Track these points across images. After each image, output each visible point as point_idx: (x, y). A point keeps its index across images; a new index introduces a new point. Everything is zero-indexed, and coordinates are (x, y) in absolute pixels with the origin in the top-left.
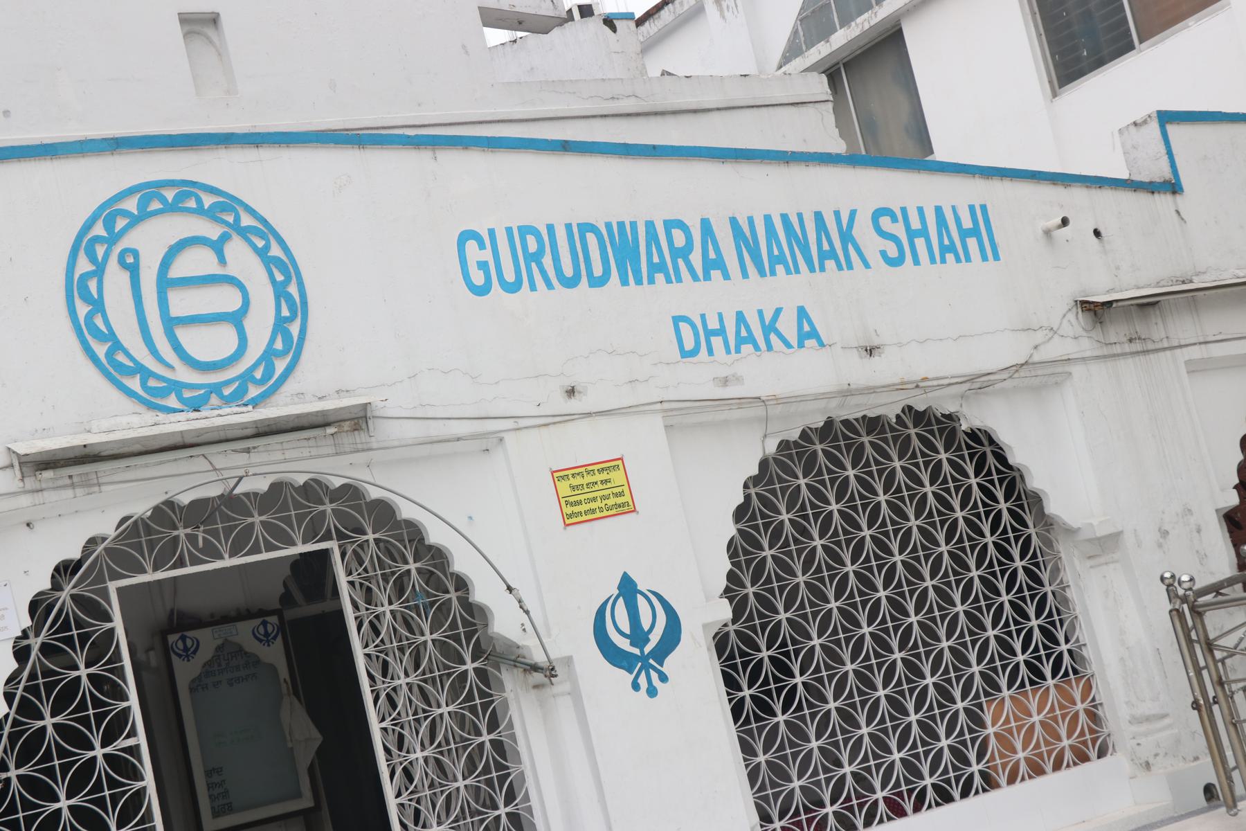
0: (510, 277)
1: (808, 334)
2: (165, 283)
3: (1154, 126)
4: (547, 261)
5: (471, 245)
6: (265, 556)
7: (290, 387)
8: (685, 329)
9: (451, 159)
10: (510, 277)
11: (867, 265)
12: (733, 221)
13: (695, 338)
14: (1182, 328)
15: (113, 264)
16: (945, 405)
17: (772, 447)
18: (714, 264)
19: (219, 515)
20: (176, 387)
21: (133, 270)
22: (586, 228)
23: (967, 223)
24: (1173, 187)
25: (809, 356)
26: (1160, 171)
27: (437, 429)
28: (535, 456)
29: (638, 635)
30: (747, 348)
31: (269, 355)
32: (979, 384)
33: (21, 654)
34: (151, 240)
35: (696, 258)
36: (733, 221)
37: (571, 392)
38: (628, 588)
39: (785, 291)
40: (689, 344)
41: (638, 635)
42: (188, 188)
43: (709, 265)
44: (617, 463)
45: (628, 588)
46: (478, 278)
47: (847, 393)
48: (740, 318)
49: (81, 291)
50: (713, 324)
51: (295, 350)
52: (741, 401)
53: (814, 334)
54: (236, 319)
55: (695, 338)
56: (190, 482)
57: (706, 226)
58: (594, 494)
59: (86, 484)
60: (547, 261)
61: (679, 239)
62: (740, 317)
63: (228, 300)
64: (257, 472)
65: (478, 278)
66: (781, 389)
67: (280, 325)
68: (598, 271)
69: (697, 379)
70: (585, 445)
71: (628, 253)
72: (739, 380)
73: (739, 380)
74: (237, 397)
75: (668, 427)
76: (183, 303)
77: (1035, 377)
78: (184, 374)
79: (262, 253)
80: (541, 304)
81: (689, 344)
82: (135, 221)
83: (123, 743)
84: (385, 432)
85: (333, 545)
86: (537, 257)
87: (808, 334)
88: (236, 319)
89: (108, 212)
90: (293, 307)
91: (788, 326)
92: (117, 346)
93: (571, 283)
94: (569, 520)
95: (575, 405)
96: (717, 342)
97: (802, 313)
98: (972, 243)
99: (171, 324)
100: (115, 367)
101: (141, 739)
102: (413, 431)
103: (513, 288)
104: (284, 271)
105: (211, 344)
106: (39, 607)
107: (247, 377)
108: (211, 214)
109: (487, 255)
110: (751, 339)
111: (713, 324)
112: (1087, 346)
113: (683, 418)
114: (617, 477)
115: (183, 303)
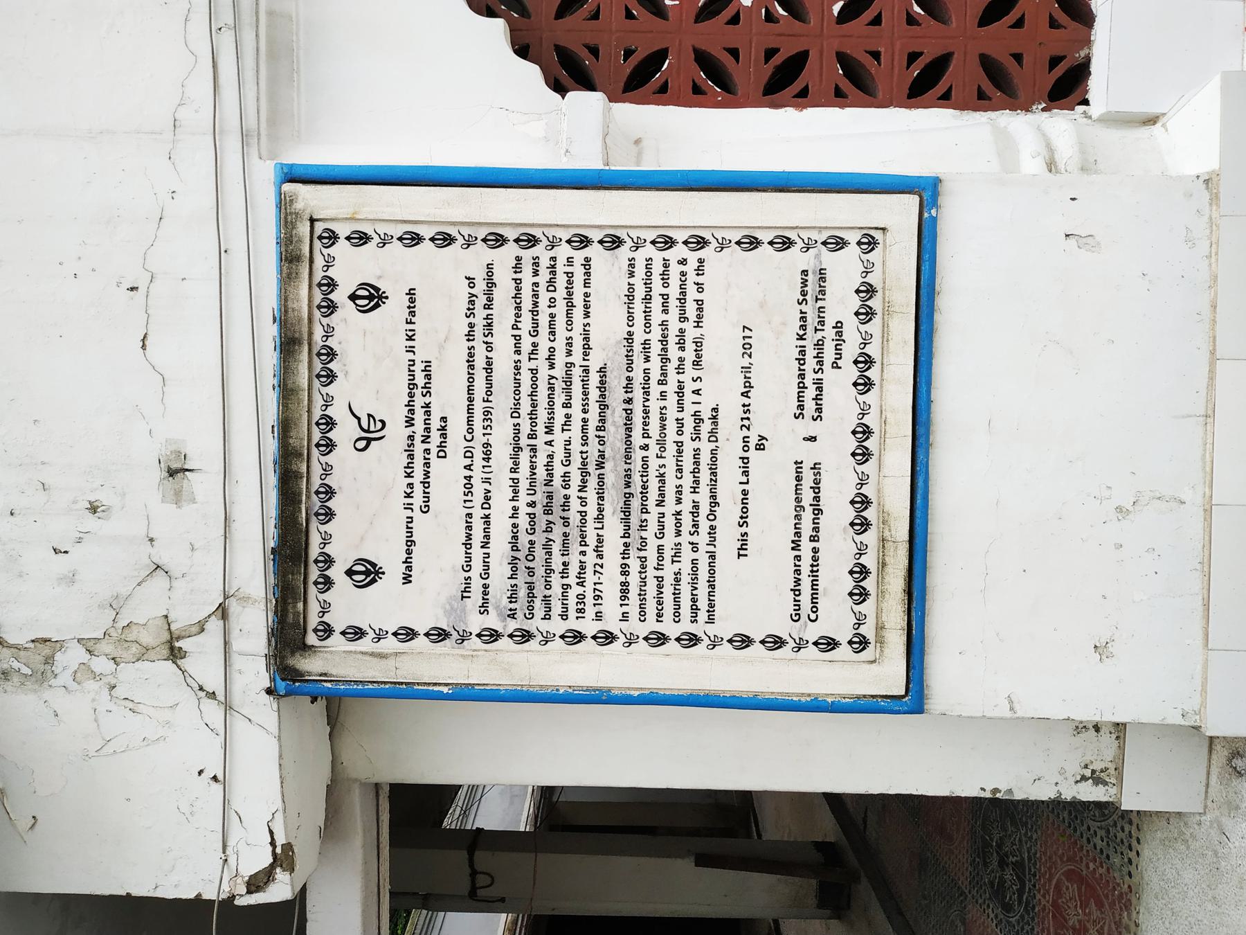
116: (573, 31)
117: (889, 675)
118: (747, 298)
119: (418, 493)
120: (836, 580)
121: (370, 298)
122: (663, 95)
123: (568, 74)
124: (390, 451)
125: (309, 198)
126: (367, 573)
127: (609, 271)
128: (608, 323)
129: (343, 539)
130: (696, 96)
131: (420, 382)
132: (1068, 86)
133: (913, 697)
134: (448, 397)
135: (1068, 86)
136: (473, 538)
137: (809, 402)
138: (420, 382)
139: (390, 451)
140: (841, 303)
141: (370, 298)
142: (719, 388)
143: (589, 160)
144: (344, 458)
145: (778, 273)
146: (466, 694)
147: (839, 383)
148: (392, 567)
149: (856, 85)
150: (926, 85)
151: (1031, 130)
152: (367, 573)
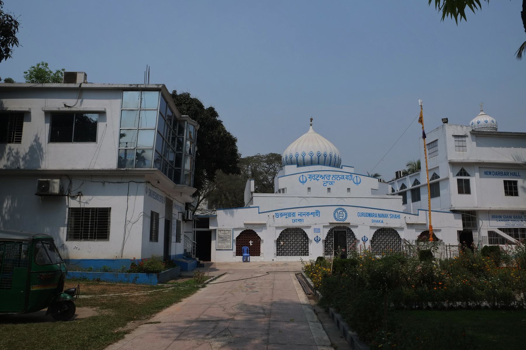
1: (382, 222)
13: (373, 221)
19: (340, 227)
24: (418, 215)
26: (417, 214)
32: (395, 228)
34: (339, 211)
39: (381, 219)
49: (334, 214)
55: (373, 221)
56: (338, 225)
64: (342, 225)
71: (370, 215)
77: (402, 229)
80: (363, 218)
100: (335, 218)
104: (346, 214)
118: (229, 244)
123: (237, 238)
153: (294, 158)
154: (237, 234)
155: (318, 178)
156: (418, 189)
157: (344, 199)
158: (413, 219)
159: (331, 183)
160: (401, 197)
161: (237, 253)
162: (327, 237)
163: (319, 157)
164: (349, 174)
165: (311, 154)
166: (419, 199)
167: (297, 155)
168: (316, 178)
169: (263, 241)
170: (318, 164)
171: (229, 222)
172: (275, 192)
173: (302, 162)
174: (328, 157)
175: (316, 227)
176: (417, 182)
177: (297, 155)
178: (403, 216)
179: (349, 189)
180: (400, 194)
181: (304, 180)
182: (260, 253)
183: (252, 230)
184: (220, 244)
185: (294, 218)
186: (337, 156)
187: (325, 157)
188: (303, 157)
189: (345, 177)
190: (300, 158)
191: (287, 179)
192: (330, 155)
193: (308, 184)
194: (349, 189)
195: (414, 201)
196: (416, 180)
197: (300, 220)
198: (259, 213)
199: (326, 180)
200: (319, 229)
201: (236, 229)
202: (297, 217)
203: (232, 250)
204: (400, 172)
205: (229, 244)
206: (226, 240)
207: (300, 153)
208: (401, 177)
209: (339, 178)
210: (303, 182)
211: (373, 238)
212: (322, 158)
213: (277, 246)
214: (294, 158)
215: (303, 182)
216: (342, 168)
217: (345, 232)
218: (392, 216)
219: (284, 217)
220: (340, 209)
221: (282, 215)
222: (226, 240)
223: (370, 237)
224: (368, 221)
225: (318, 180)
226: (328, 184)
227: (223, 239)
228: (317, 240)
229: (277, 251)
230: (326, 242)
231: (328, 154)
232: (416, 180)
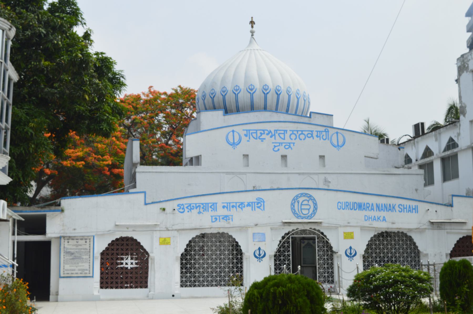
0: (343, 208)
1: (384, 219)
2: (302, 204)
3: (451, 197)
4: (349, 207)
5: (339, 204)
6: (308, 236)
7: (314, 218)
8: (366, 217)
9: (339, 193)
10: (343, 208)
11: (396, 211)
12: (377, 204)
13: (367, 218)
14: (448, 227)
15: (296, 202)
16: (405, 232)
17: (376, 233)
18: (372, 209)
19: (304, 231)
20: (301, 216)
21: (298, 203)
22: (355, 203)
23: (414, 207)
24: (451, 206)
25: (384, 222)
27: (330, 225)
28: (341, 231)
29: (351, 254)
30: (375, 221)
31: (312, 214)
32: (410, 230)
33: (280, 242)
34: (301, 200)
35: (370, 208)
36: (377, 204)
37: (349, 223)
38: (351, 248)
39: (382, 214)
40: (366, 219)
41: (351, 254)
42: (306, 194)
43: (371, 209)
44: (352, 233)
45: (351, 248)
46: (339, 208)
47: (388, 228)
48: (375, 217)
49: (293, 204)
50: (370, 217)
51: (315, 214)
52: (372, 227)
53: (385, 220)
54: (309, 209)
55: (367, 218)
56: (301, 227)
57: (372, 204)
58: (348, 236)
59: (289, 226)
60: (349, 207)
61: (368, 205)
62: (375, 217)
63: (308, 207)
64: (307, 227)
65: (339, 208)
66: (378, 227)
67: (314, 211)
68: (356, 208)
69: (367, 224)
70: (349, 230)
71: (360, 206)
72: (372, 224)
73: (372, 224)
74: (307, 218)
75: (361, 229)
76: (303, 207)
78: (302, 215)
79: (313, 202)
80: (347, 212)
81: (366, 219)
82: (300, 197)
83: (289, 253)
84: (323, 225)
85: (316, 236)
86: (348, 206)
87: (384, 219)
88: (309, 209)
89: (297, 196)
90: (316, 208)
91: (381, 219)
92: (295, 211)
93: (351, 209)
94: (345, 238)
95: (349, 225)
96: (370, 219)
97: (384, 217)
98: (414, 211)
99: (301, 209)
100: (294, 213)
101: (291, 253)
102: (327, 225)
103: (344, 209)
105: (305, 212)
106: (283, 238)
107: (309, 216)
108: (308, 197)
109: (341, 205)
110: (375, 219)
111: (370, 217)
112: (430, 227)
113: (363, 229)
114: (352, 234)
115: (303, 207)
116: (105, 254)
117: (62, 275)
118: (86, 266)
119: (73, 245)
120: (68, 272)
121: (86, 242)
122: (101, 260)
123: (102, 254)
124: (76, 243)
125: (92, 238)
126: (68, 242)
127: (88, 257)
128: (84, 257)
129: (70, 241)
130: (101, 262)
131: (81, 245)
132: (101, 287)
133: (60, 277)
134: (80, 247)
135: (101, 287)
136: (71, 249)
137: (79, 270)
138: (81, 245)
139: (76, 243)
140: (86, 272)
141: (86, 242)
142: (80, 264)
143: (95, 255)
144: (76, 241)
145: (88, 268)
146: (60, 249)
147: (80, 272)
148: (69, 244)
149: (102, 273)
150: (102, 278)
151: (98, 285)
152: (68, 242)
153: (218, 98)
154: (101, 245)
155: (263, 136)
156: (455, 156)
157: (315, 177)
158: (441, 215)
159: (289, 146)
160: (422, 171)
161: (101, 283)
162: (279, 251)
163: (266, 95)
164: (323, 129)
165: (251, 90)
166: (456, 176)
167: (224, 92)
168: (259, 136)
169: (153, 259)
170: (265, 109)
171: (84, 222)
172: (184, 162)
173: (234, 107)
174: (284, 97)
175: (257, 230)
176: (452, 144)
177: (224, 92)
178: (422, 207)
179: (322, 157)
180: (421, 167)
181: (236, 140)
182: (146, 282)
183: (132, 239)
184: (67, 267)
185: (214, 213)
186: (301, 93)
187: (278, 95)
188: (236, 96)
189: (315, 134)
190: (230, 98)
191: (204, 138)
192: (288, 92)
193: (243, 148)
194: (322, 157)
195: (445, 178)
196: (451, 140)
197: (226, 218)
198: (146, 204)
199: (278, 140)
200: (264, 234)
201: (102, 235)
202: (221, 212)
203: (93, 277)
204: (422, 124)
205: (86, 266)
206: (80, 258)
207: (229, 87)
208: (423, 134)
209: (302, 137)
210: (234, 144)
211: (366, 251)
212: (271, 98)
213: (182, 268)
214: (218, 98)
215: (234, 144)
216: (310, 117)
217: (313, 239)
218: (403, 209)
219: (195, 211)
220: (305, 195)
221: (190, 207)
222: (80, 258)
223: (361, 248)
224: (358, 217)
225: (263, 140)
226: (282, 148)
227: (74, 256)
228: (259, 256)
229: (182, 277)
230: (279, 258)
231: (283, 89)
232: (451, 140)
